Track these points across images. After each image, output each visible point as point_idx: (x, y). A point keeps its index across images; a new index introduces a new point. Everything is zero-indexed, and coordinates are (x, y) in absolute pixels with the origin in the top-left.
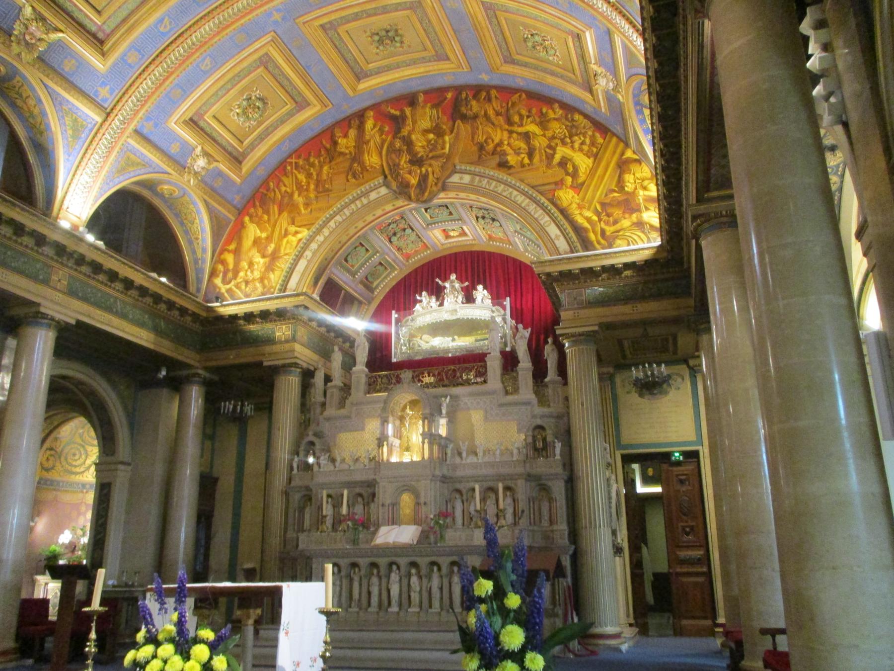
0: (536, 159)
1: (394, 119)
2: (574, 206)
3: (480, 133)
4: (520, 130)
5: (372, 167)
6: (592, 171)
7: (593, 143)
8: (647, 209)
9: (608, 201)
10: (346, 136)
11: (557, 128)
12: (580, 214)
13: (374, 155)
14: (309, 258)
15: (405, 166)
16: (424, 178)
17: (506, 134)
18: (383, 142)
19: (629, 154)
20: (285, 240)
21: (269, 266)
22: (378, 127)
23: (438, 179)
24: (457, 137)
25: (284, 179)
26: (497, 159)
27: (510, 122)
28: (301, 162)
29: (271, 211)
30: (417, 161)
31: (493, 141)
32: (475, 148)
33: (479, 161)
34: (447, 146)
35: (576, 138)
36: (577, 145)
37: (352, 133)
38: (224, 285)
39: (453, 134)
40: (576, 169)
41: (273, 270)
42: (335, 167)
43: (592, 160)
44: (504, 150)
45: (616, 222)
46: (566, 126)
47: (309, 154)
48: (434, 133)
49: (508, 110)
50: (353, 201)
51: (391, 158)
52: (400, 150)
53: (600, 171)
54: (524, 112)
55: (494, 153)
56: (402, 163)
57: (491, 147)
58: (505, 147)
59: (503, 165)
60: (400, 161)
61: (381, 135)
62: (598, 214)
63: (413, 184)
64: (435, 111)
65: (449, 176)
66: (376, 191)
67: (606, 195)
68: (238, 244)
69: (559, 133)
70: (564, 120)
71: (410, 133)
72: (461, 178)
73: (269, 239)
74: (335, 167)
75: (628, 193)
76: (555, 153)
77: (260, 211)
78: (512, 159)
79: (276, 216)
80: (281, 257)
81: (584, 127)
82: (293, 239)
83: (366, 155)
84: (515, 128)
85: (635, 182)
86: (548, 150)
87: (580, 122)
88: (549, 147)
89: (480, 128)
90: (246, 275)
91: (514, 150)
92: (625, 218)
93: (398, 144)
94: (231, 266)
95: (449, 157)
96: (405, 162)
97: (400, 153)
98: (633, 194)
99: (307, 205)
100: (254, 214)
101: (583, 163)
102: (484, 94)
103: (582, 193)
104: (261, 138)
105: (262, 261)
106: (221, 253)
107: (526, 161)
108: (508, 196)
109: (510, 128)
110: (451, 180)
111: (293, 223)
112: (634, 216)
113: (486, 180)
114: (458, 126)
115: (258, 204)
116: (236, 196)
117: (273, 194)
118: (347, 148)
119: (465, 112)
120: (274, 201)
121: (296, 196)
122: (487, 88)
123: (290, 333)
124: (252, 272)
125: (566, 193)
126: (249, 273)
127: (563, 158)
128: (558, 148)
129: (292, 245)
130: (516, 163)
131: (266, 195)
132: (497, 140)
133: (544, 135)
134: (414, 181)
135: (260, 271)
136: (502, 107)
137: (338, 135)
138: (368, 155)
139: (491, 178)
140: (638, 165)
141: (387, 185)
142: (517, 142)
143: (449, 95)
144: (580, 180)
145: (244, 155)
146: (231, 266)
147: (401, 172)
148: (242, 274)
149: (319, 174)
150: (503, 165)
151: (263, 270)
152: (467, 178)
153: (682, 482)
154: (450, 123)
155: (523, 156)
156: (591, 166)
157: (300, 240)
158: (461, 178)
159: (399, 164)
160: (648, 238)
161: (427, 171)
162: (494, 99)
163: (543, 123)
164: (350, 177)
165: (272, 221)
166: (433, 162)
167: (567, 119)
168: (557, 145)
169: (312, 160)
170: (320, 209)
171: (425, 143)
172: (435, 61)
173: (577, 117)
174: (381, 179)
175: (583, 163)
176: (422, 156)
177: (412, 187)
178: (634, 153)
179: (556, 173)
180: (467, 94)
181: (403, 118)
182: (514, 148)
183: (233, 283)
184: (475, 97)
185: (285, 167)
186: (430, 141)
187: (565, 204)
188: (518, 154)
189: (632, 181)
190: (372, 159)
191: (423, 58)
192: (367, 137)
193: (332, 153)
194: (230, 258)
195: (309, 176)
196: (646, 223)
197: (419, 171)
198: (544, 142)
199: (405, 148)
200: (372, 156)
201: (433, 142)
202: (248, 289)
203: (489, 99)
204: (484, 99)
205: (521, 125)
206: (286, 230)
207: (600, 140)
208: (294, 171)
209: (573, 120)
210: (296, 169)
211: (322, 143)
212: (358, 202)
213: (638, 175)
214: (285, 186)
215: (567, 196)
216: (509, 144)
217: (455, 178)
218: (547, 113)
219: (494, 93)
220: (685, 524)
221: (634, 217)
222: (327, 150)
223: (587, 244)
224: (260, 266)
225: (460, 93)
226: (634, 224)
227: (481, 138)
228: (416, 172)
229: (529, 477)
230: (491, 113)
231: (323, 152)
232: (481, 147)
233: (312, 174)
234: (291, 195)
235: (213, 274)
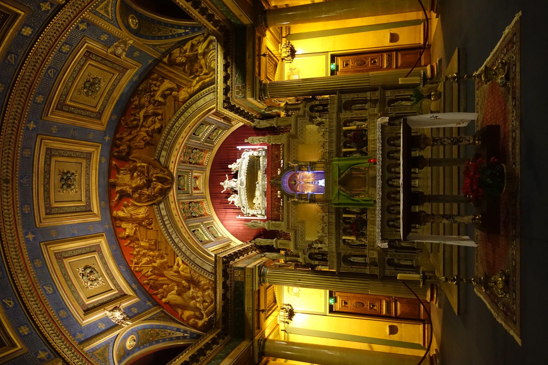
0: (160, 111)
1: (120, 198)
2: (189, 90)
3: (140, 144)
4: (142, 121)
5: (147, 213)
6: (172, 80)
7: (157, 80)
8: (197, 50)
9: (189, 72)
12: (194, 87)
13: (140, 211)
14: (195, 257)
15: (150, 191)
16: (159, 179)
17: (143, 129)
18: (133, 205)
19: (165, 60)
20: (181, 273)
21: (196, 285)
22: (124, 208)
23: (161, 171)
25: (143, 272)
26: (155, 135)
27: (137, 126)
28: (135, 260)
29: (162, 282)
31: (145, 137)
32: (147, 148)
34: (143, 164)
35: (152, 89)
36: (156, 89)
37: (124, 225)
38: (203, 318)
39: (137, 161)
40: (169, 89)
41: (199, 282)
42: (142, 237)
43: (165, 80)
44: (151, 130)
45: (201, 67)
46: (144, 94)
47: (132, 254)
48: (134, 173)
49: (129, 128)
50: (165, 226)
51: (144, 200)
52: (140, 194)
53: (172, 76)
54: (132, 118)
55: (152, 136)
56: (148, 193)
58: (150, 129)
59: (160, 131)
60: (146, 194)
61: (129, 206)
62: (196, 77)
63: (161, 186)
64: (121, 172)
65: (161, 164)
66: (161, 210)
67: (186, 72)
68: (179, 307)
69: (147, 98)
70: (141, 96)
71: (131, 188)
72: (163, 157)
73: (179, 284)
74: (142, 237)
75: (186, 61)
76: (158, 101)
77: (160, 290)
78: (157, 126)
79: (166, 279)
80: (191, 276)
81: (147, 84)
82: (182, 266)
83: (139, 216)
84: (140, 124)
85: (181, 57)
86: (156, 105)
87: (143, 87)
88: (154, 104)
89: (136, 144)
90: (199, 302)
91: (152, 125)
92: (200, 62)
93: (137, 195)
94: (192, 313)
95: (149, 164)
96: (147, 191)
97: (143, 194)
98: (188, 58)
99: (162, 257)
100: (162, 294)
101: (167, 84)
103: (183, 86)
104: (113, 279)
105: (192, 290)
106: (183, 320)
107: (160, 117)
108: (178, 128)
109: (140, 126)
110: (163, 163)
111: (172, 267)
112: (199, 57)
113: (166, 141)
114: (133, 157)
115: (155, 292)
116: (147, 304)
117: (151, 281)
118: (132, 229)
119: (125, 153)
121: (154, 264)
122: (114, 139)
123: (239, 271)
124: (198, 297)
125: (181, 95)
126: (198, 300)
127: (161, 96)
128: (156, 99)
129: (185, 268)
130: (160, 123)
131: (151, 286)
132: (145, 134)
133: (147, 107)
134: (159, 186)
135: (198, 291)
136: (127, 131)
137: (123, 235)
138: (140, 215)
139: (166, 139)
140: (172, 55)
142: (148, 123)
143: (114, 163)
144: (176, 87)
145: (120, 290)
146: (192, 313)
147: (153, 193)
148: (198, 305)
150: (160, 131)
151: (197, 289)
152: (164, 153)
153: (347, 65)
154: (130, 162)
155: (156, 119)
156: (169, 81)
157: (183, 262)
158: (163, 157)
159: (149, 195)
160: (213, 49)
161: (155, 177)
162: (122, 136)
163: (140, 107)
164: (150, 228)
165: (168, 282)
166: (151, 173)
167: (141, 94)
168: (154, 100)
169: (135, 253)
170: (166, 248)
171: (139, 178)
172: (90, 162)
173: (140, 88)
175: (167, 84)
176: (146, 180)
177: (163, 187)
178: (165, 57)
179: (170, 101)
180: (115, 152)
181: (121, 191)
182: (151, 124)
183: (203, 312)
184: (118, 147)
185: (136, 271)
186: (138, 174)
187: (187, 95)
188: (155, 122)
189: (180, 58)
191: (86, 167)
192: (129, 215)
194: (187, 313)
195: (144, 255)
196: (204, 51)
197: (154, 182)
198: (151, 106)
199: (139, 191)
200: (140, 212)
201: (139, 173)
202: (208, 301)
203: (121, 139)
204: (120, 141)
205: (139, 120)
206: (175, 272)
208: (140, 265)
209: (142, 91)
210: (139, 264)
211: (127, 246)
212: (166, 223)
213: (178, 55)
214: (148, 272)
216: (149, 127)
217: (162, 160)
218: (135, 105)
219: (118, 136)
220: (370, 63)
222: (132, 242)
224: (195, 291)
225: (115, 156)
226: (204, 58)
227: (143, 143)
228: (155, 184)
229: (339, 111)
230: (129, 138)
231: (132, 245)
232: (147, 144)
233: (144, 253)
234: (154, 267)
235: (194, 326)
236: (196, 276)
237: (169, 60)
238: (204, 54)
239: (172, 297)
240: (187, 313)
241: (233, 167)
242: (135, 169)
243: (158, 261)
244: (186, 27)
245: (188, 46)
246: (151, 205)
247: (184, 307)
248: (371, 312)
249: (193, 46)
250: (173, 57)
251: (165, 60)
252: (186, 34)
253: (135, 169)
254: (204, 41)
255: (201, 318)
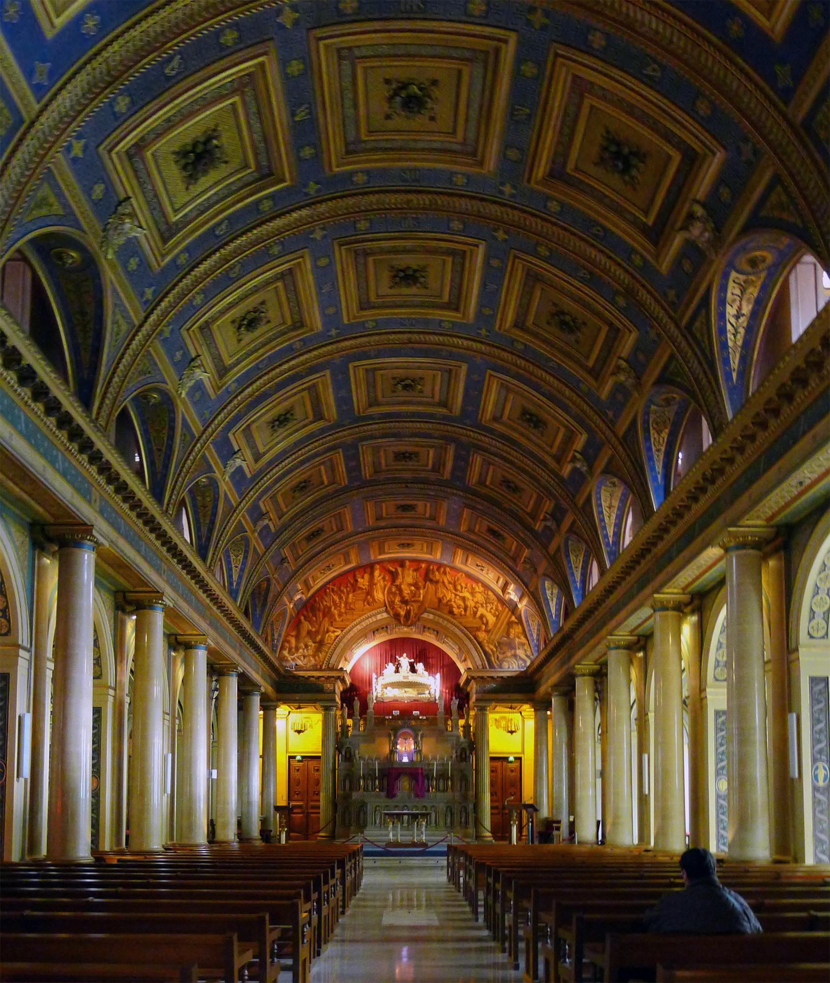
0: (468, 613)
1: (391, 572)
4: (461, 595)
7: (497, 610)
10: (363, 577)
11: (480, 597)
16: (408, 613)
18: (385, 586)
24: (427, 592)
25: (326, 598)
27: (456, 590)
30: (404, 602)
33: (438, 608)
36: (489, 609)
37: (367, 576)
40: (487, 622)
45: (504, 653)
50: (367, 618)
54: (464, 585)
55: (447, 605)
57: (445, 601)
59: (451, 612)
62: (495, 646)
73: (317, 632)
77: (311, 615)
78: (456, 610)
82: (333, 635)
93: (394, 590)
95: (422, 603)
98: (514, 639)
99: (340, 615)
102: (442, 570)
107: (463, 613)
120: (319, 610)
132: (448, 598)
134: (403, 613)
141: (387, 611)
143: (423, 566)
146: (294, 646)
148: (301, 651)
149: (347, 598)
163: (473, 593)
170: (348, 620)
173: (490, 593)
174: (384, 609)
181: (397, 573)
184: (438, 570)
185: (325, 591)
187: (481, 640)
190: (379, 595)
193: (355, 587)
195: (340, 598)
198: (473, 604)
207: (500, 608)
215: (482, 635)
217: (425, 615)
219: (448, 569)
221: (513, 652)
222: (352, 585)
223: (491, 665)
227: (441, 596)
230: (446, 581)
234: (330, 608)
236: (325, 649)
237: (513, 622)
238: (515, 656)
239: (306, 626)
240: (293, 641)
241: (420, 667)
242: (418, 588)
243: (336, 612)
244: (538, 640)
245: (523, 640)
246: (385, 605)
247: (297, 637)
248: (292, 792)
249: (523, 644)
250: (515, 626)
251: (513, 618)
252: (533, 640)
253: (418, 588)
254: (527, 656)
255: (289, 652)
